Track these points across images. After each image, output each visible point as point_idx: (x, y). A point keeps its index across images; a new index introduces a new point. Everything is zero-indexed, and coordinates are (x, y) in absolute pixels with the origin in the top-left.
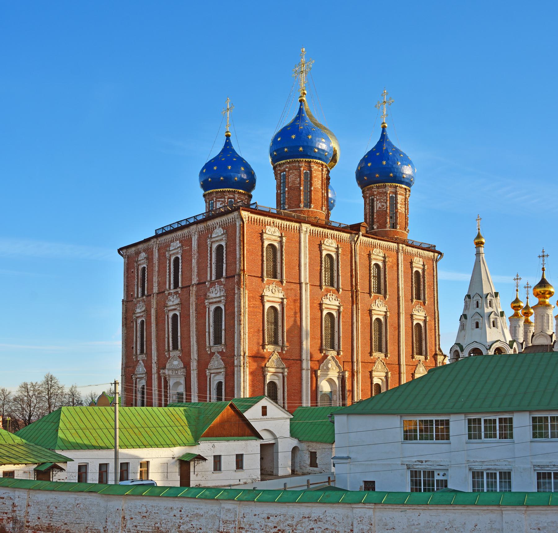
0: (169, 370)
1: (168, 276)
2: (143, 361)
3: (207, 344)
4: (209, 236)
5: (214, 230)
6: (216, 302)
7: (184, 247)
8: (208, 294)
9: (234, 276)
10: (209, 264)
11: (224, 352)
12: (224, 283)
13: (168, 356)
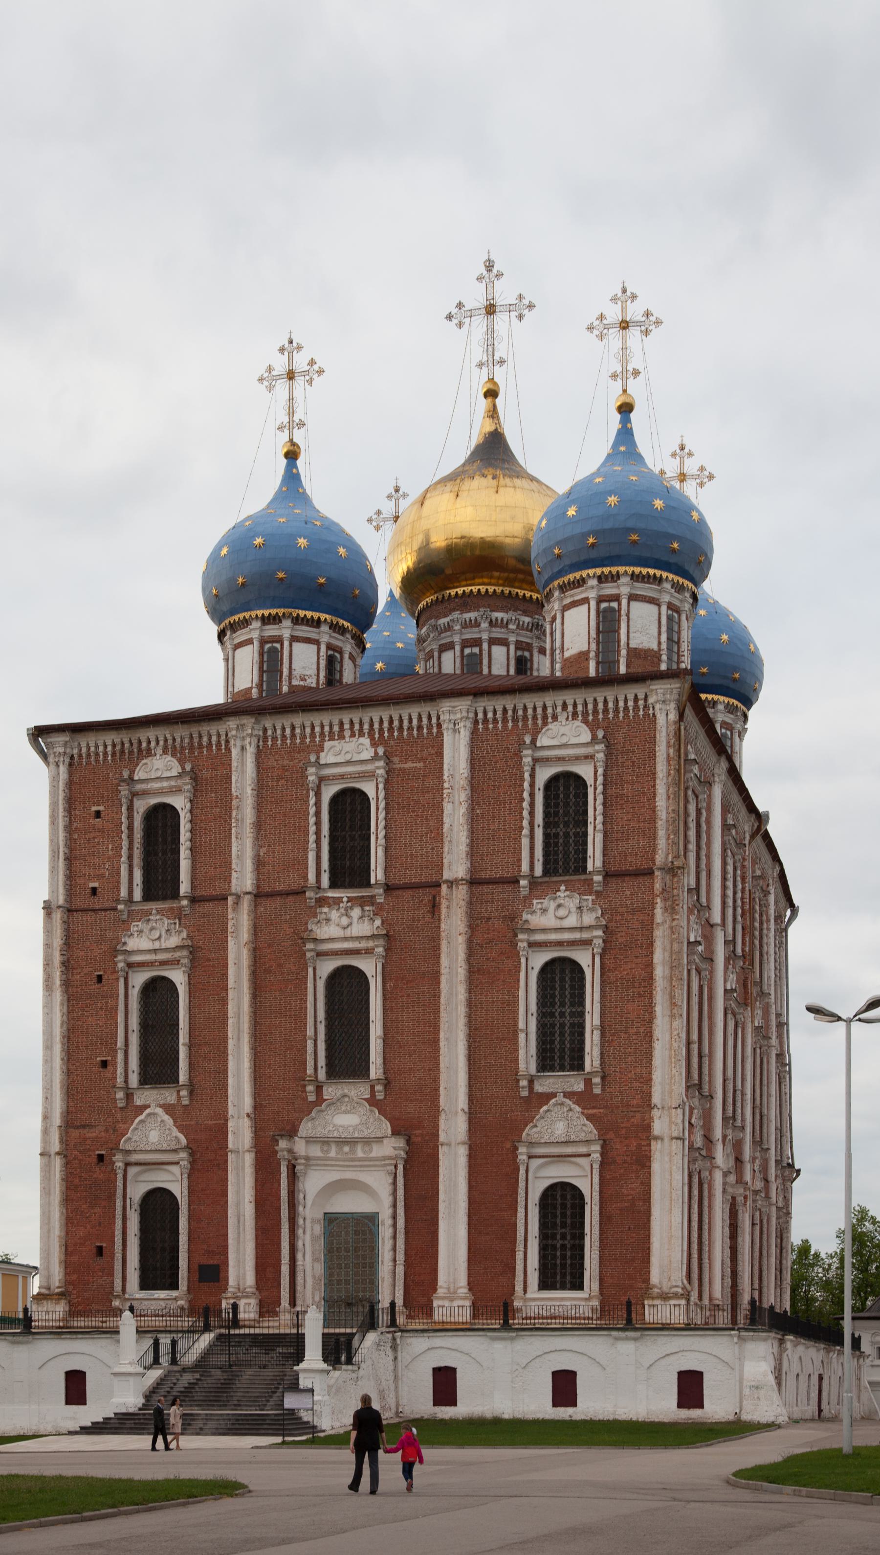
0: (309, 1140)
1: (312, 845)
2: (168, 1109)
3: (522, 1066)
4: (528, 739)
5: (545, 723)
6: (560, 944)
7: (396, 760)
8: (525, 916)
9: (650, 873)
10: (525, 823)
11: (598, 1095)
12: (600, 888)
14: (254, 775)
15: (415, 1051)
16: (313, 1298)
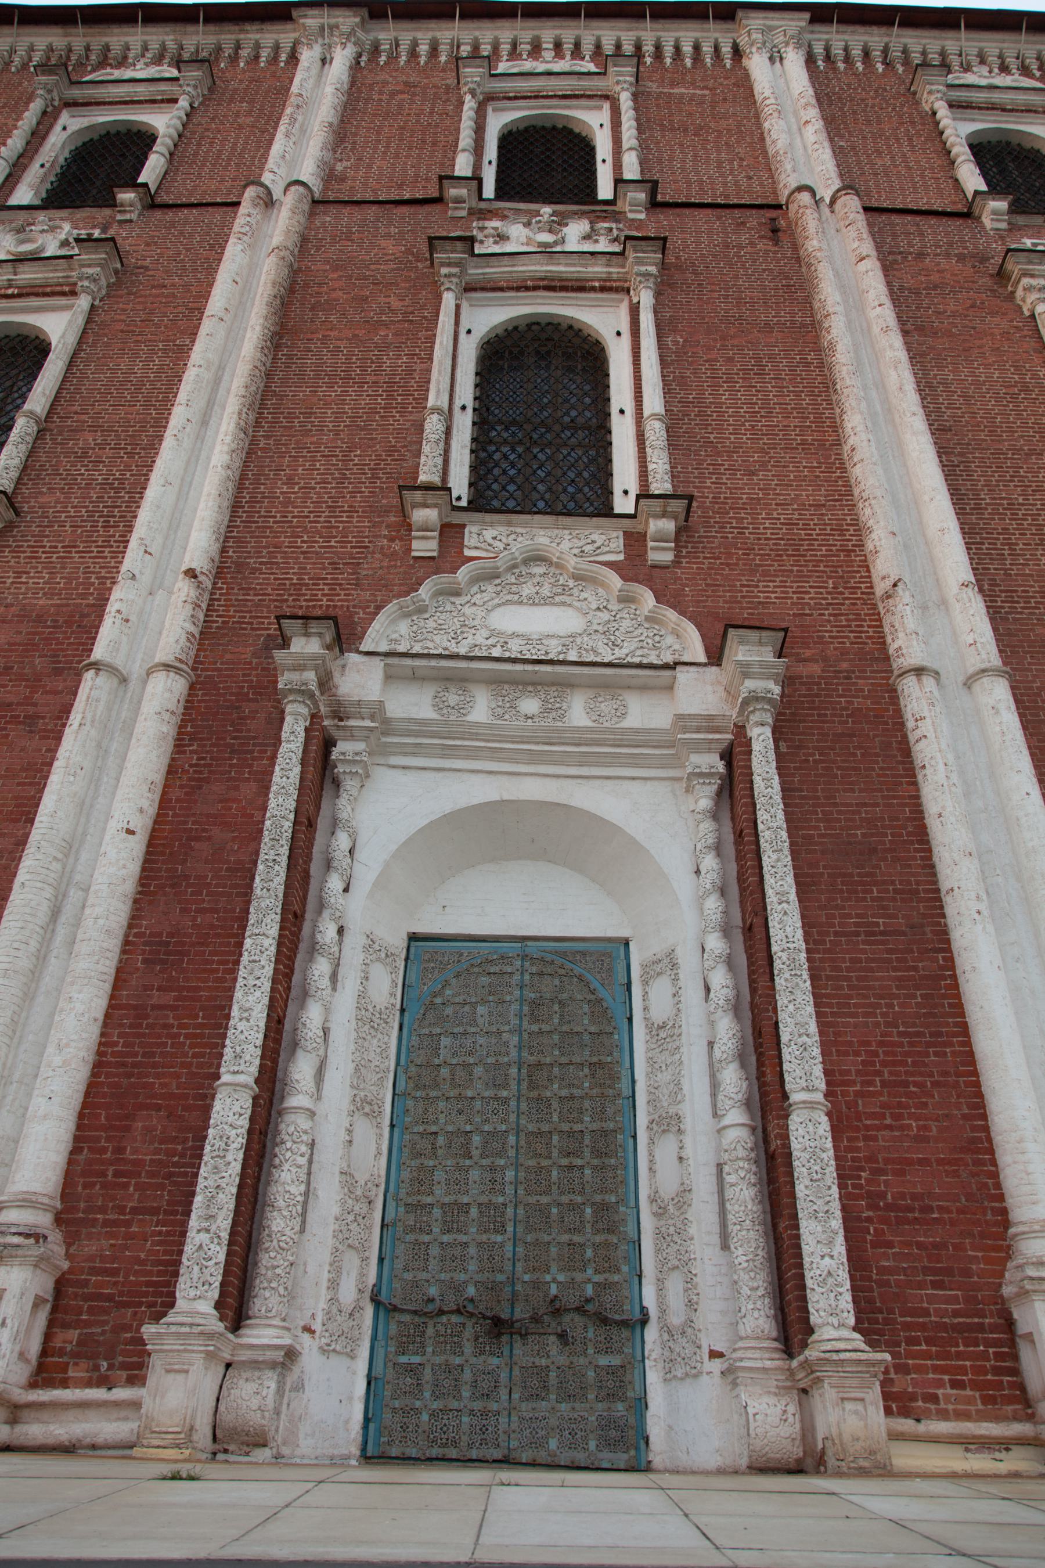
13: (425, 546)
14: (345, 78)
15: (764, 465)
16: (334, 1284)
